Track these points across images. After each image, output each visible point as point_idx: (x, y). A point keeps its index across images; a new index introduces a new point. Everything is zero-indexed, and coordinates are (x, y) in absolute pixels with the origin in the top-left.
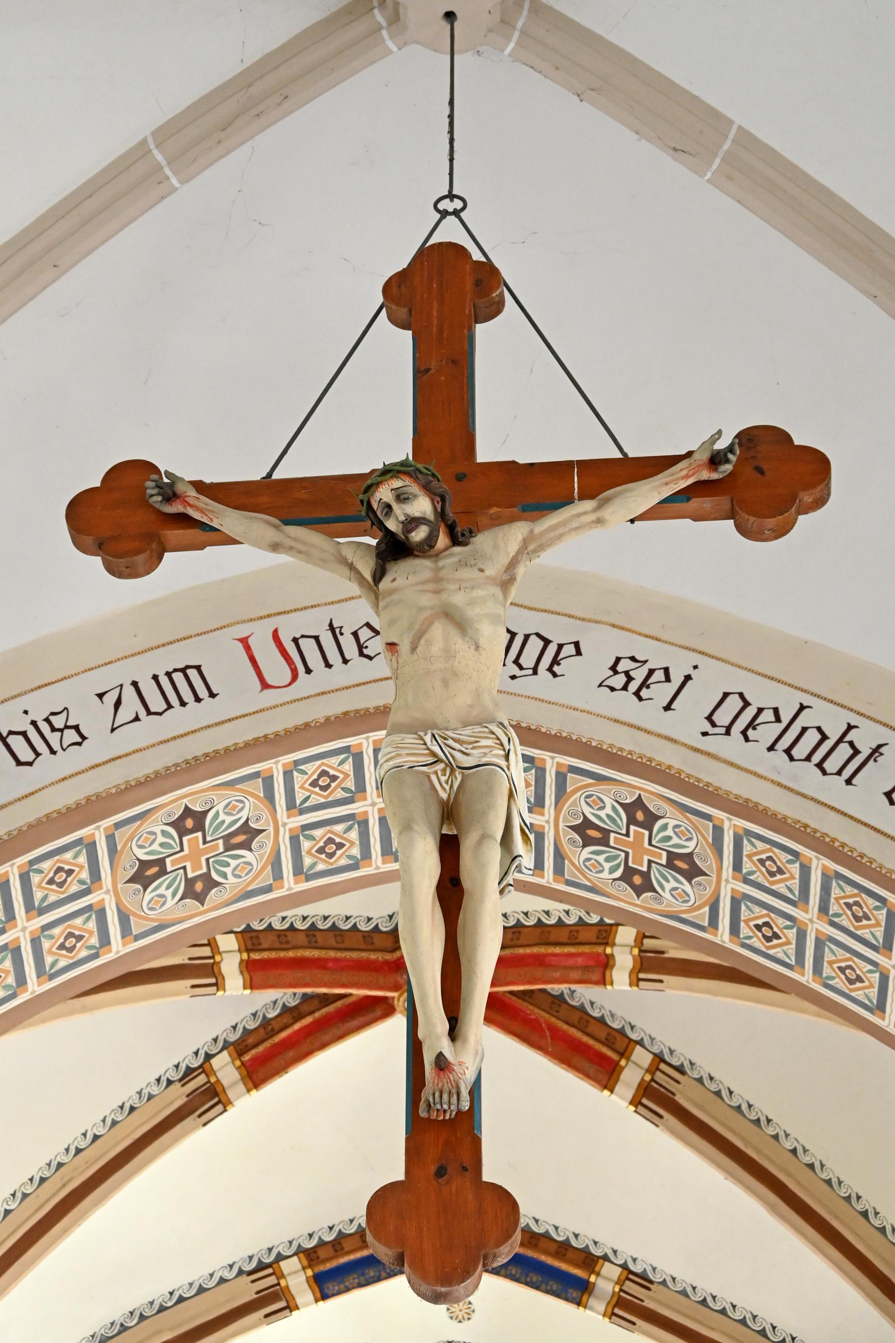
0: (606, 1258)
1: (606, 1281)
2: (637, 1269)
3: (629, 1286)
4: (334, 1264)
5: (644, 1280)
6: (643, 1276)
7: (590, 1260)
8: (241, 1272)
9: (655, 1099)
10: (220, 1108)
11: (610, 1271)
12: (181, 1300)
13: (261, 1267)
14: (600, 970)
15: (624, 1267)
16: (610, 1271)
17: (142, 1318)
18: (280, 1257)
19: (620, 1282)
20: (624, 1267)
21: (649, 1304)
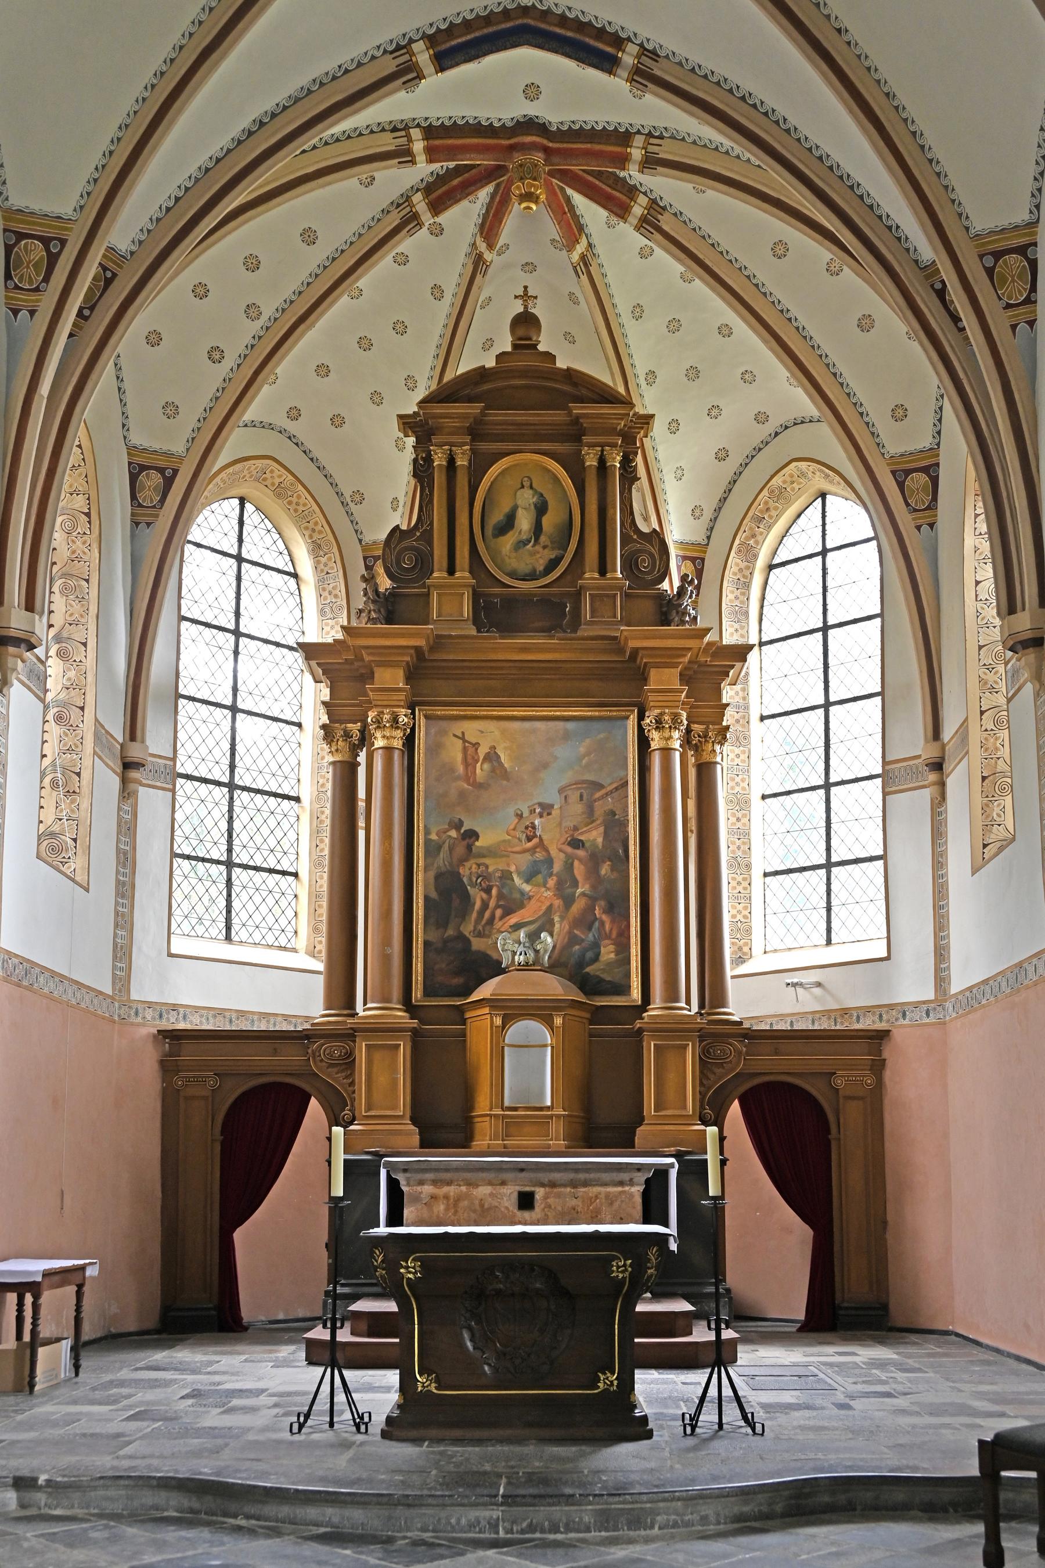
0: (629, 39)
1: (628, 58)
2: (650, 47)
3: (644, 58)
4: (448, 45)
5: (654, 55)
6: (654, 52)
7: (618, 42)
8: (385, 52)
9: (649, 224)
10: (418, 227)
11: (632, 49)
12: (347, 71)
13: (399, 48)
14: (623, 161)
15: (641, 45)
16: (632, 49)
17: (322, 84)
18: (411, 41)
19: (638, 57)
20: (641, 45)
21: (657, 72)
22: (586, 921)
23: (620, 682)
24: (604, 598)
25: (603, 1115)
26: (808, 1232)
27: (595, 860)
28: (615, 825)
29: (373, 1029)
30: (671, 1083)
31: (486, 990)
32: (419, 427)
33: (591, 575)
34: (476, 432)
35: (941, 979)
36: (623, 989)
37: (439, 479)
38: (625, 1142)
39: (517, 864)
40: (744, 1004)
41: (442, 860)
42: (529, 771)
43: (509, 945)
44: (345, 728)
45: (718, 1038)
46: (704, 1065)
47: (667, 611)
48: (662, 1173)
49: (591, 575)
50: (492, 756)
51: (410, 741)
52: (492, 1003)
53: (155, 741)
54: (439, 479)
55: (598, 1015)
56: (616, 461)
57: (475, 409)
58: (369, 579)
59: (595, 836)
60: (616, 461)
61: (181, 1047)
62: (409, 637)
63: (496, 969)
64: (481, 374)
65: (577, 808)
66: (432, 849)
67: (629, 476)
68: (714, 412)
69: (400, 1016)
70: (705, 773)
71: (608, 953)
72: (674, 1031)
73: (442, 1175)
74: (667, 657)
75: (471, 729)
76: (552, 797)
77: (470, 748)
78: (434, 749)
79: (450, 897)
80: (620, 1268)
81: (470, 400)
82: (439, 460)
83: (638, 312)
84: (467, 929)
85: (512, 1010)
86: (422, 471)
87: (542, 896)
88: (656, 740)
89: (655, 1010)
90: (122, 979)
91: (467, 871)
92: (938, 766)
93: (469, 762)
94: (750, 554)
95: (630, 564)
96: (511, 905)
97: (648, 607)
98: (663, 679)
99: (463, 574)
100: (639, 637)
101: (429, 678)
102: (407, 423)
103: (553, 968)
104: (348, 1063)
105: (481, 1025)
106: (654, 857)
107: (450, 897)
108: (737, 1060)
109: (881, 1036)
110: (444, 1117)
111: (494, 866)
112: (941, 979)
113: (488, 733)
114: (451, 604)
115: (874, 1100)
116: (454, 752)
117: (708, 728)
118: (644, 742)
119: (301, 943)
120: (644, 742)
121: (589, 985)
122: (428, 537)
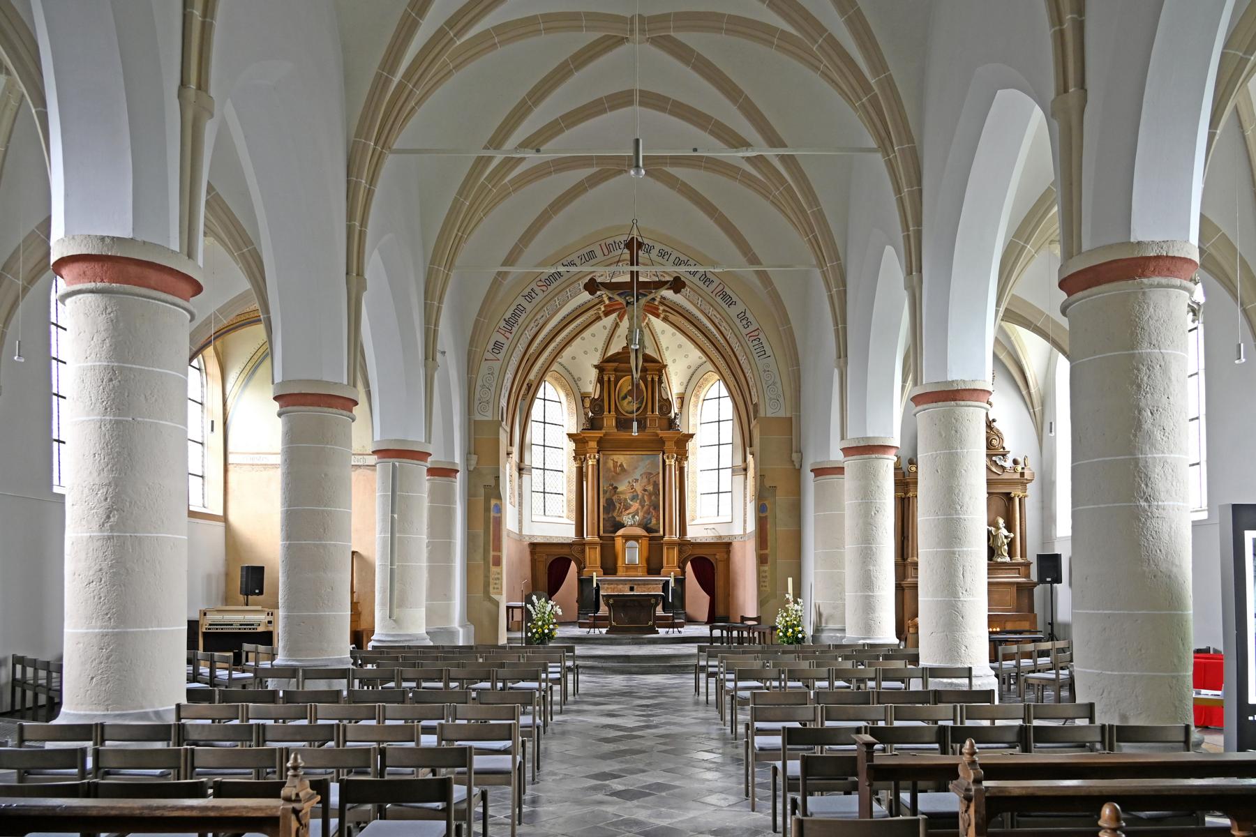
22: (648, 512)
23: (658, 445)
24: (653, 420)
25: (654, 567)
26: (708, 598)
27: (650, 495)
28: (656, 485)
29: (591, 544)
30: (671, 558)
31: (620, 532)
32: (600, 368)
33: (649, 413)
34: (616, 370)
35: (745, 529)
36: (658, 531)
37: (606, 385)
38: (658, 573)
39: (628, 496)
40: (693, 533)
41: (608, 495)
42: (633, 475)
43: (627, 519)
44: (579, 455)
45: (683, 544)
46: (680, 552)
47: (671, 424)
48: (668, 582)
49: (649, 413)
50: (621, 465)
51: (598, 461)
52: (623, 536)
53: (527, 462)
54: (606, 385)
55: (651, 539)
56: (656, 379)
57: (615, 364)
58: (586, 414)
59: (650, 488)
60: (656, 379)
61: (534, 546)
62: (598, 434)
63: (623, 526)
64: (618, 353)
65: (645, 480)
66: (605, 492)
67: (660, 382)
68: (686, 356)
69: (597, 539)
70: (681, 470)
71: (654, 521)
72: (671, 544)
73: (610, 582)
74: (670, 439)
75: (615, 457)
76: (638, 477)
77: (615, 463)
78: (605, 463)
79: (610, 506)
80: (653, 601)
81: (614, 361)
82: (606, 378)
83: (663, 332)
84: (615, 514)
85: (627, 538)
86: (600, 380)
87: (635, 506)
88: (667, 462)
89: (666, 538)
90: (520, 530)
91: (615, 498)
92: (745, 470)
93: (615, 467)
94: (697, 396)
95: (660, 408)
96: (627, 507)
97: (665, 422)
98: (669, 445)
99: (613, 413)
100: (663, 434)
101: (604, 446)
102: (596, 367)
103: (639, 525)
104: (583, 551)
105: (619, 542)
106: (666, 494)
107: (610, 506)
108: (689, 551)
109: (730, 544)
110: (609, 567)
111: (622, 497)
112: (745, 529)
113: (621, 458)
114: (609, 421)
115: (727, 561)
116: (611, 464)
117: (682, 455)
118: (664, 462)
119: (564, 515)
120: (664, 462)
121: (648, 530)
122: (603, 400)
